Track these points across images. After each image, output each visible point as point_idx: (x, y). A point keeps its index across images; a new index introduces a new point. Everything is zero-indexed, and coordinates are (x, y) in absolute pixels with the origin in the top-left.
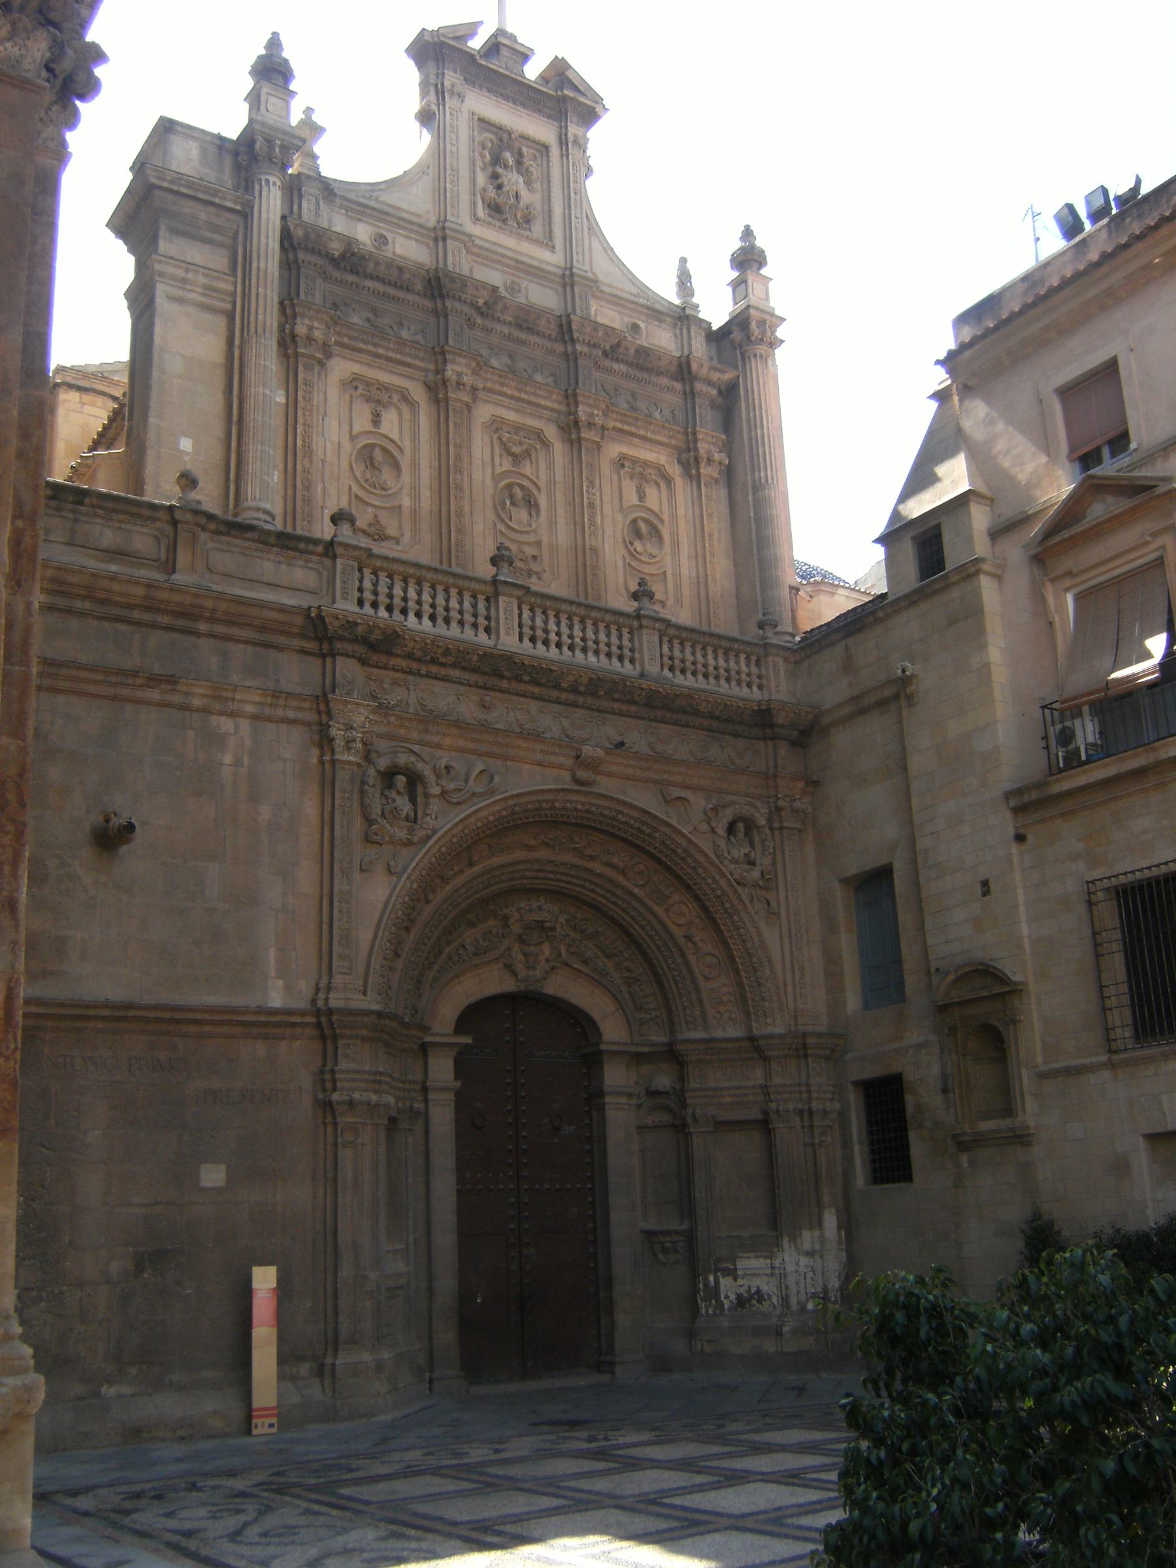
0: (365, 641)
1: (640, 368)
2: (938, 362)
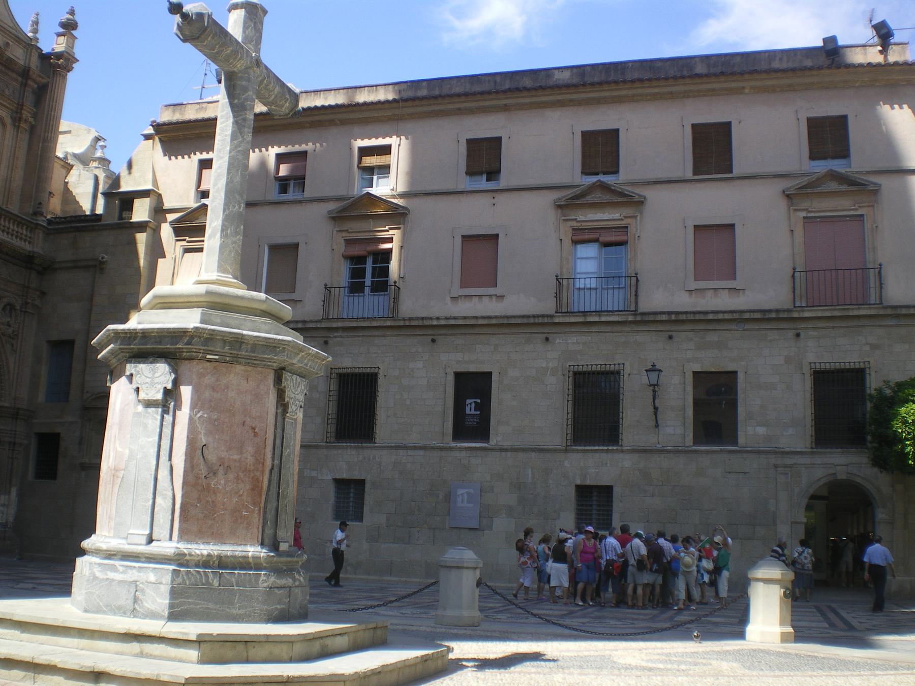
1: (6, 67)
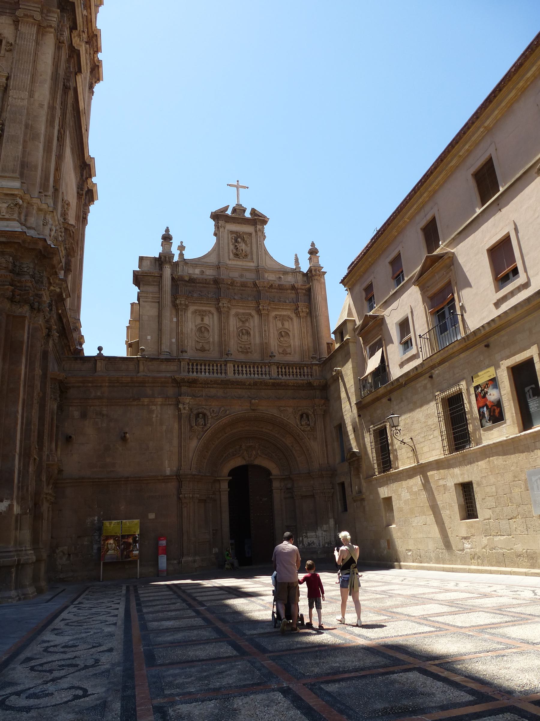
0: (188, 382)
2: (340, 283)
